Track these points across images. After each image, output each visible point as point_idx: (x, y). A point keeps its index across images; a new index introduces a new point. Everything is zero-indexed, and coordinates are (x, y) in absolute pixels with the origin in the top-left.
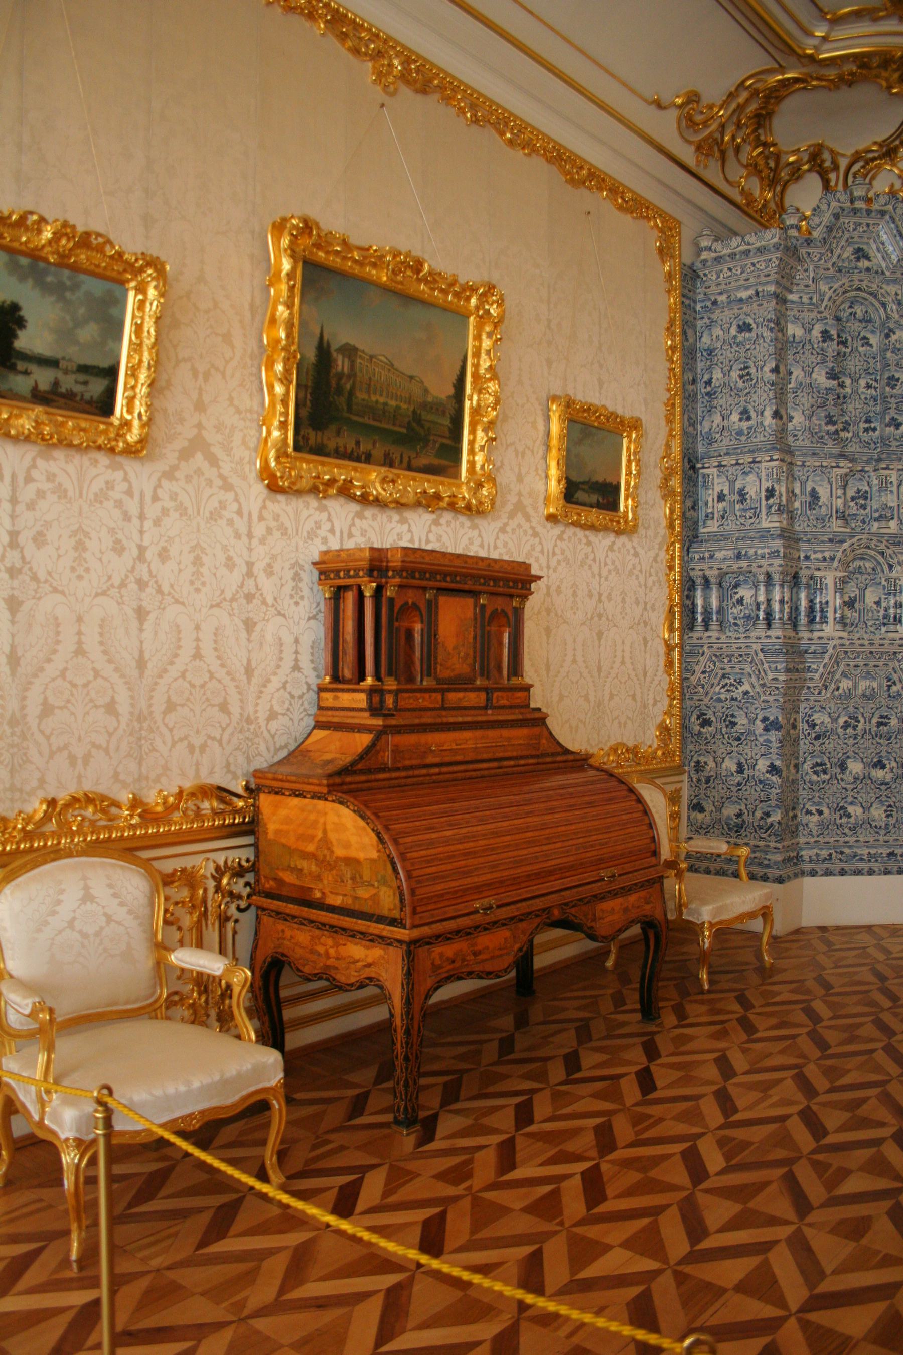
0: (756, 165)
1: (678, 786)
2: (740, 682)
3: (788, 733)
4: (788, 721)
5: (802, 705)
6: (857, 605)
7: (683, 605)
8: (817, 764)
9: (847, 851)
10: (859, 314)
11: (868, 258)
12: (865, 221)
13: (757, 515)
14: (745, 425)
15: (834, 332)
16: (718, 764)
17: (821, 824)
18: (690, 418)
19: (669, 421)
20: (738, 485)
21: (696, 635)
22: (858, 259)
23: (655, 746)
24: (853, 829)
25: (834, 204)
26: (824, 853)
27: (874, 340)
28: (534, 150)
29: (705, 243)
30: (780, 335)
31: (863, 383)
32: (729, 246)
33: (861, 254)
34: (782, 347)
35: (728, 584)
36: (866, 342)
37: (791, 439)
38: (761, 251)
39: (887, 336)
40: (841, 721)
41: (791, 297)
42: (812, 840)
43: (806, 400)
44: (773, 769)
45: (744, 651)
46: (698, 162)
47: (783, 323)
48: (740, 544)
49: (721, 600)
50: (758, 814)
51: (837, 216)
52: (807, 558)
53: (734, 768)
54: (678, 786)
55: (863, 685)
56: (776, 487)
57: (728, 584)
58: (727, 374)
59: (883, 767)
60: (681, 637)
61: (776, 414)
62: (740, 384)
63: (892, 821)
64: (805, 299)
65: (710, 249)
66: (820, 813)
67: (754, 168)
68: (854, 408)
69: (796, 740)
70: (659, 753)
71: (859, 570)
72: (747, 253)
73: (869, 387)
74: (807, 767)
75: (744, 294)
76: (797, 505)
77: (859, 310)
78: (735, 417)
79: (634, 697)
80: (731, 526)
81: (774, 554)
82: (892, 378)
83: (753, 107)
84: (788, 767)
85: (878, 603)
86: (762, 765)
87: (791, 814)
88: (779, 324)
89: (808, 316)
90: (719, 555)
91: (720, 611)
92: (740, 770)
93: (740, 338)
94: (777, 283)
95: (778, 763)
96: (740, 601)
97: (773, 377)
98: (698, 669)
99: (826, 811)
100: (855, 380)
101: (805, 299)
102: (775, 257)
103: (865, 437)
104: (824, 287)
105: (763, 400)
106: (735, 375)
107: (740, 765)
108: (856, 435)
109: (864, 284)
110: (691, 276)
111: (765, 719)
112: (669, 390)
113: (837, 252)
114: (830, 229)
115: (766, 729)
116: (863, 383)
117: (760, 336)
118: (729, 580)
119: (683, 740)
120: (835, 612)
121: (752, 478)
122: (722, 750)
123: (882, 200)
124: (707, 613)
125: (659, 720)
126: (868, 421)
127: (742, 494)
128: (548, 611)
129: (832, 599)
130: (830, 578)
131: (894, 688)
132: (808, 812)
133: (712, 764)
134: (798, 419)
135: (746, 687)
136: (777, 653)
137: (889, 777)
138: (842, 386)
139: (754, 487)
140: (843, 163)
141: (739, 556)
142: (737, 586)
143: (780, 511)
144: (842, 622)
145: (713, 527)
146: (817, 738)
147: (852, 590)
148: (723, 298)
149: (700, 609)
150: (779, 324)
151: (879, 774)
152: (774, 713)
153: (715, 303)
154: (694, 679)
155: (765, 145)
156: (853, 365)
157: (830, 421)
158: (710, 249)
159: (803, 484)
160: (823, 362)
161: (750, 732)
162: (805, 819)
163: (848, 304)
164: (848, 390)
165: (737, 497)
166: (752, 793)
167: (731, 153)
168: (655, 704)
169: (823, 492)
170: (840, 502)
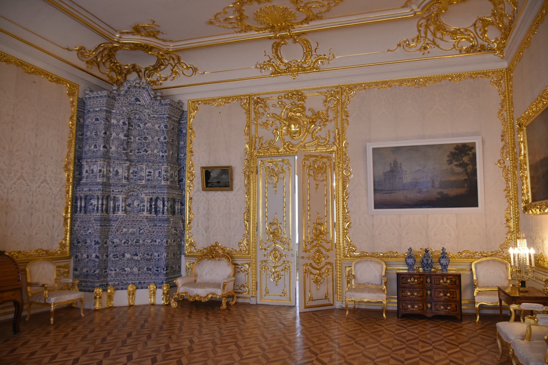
0: (112, 68)
1: (68, 263)
2: (88, 230)
3: (103, 245)
4: (103, 241)
5: (110, 237)
6: (131, 206)
7: (72, 205)
8: (114, 255)
9: (124, 282)
10: (137, 117)
11: (140, 101)
12: (138, 90)
13: (96, 178)
14: (95, 149)
15: (127, 123)
16: (82, 256)
17: (116, 274)
18: (79, 147)
19: (69, 147)
20: (92, 168)
21: (76, 214)
22: (136, 101)
23: (58, 249)
24: (127, 275)
25: (129, 84)
26: (117, 283)
27: (142, 125)
28: (10, 62)
29: (87, 92)
30: (108, 123)
31: (137, 138)
32: (102, 93)
33: (137, 100)
34: (108, 127)
35: (87, 198)
36: (139, 126)
37: (111, 154)
38: (101, 97)
39: (145, 125)
40: (123, 241)
41: (113, 111)
42: (112, 279)
43: (116, 143)
44: (97, 257)
45: (89, 220)
46: (88, 67)
47: (109, 119)
48: (91, 186)
49: (85, 204)
50: (92, 271)
51: (129, 88)
52: (113, 191)
53: (86, 257)
54: (68, 263)
55: (131, 230)
56: (102, 169)
57: (87, 198)
58: (91, 133)
59: (137, 255)
60: (71, 215)
61: (104, 147)
62: (95, 137)
63: (140, 272)
64: (118, 112)
65: (88, 94)
66: (116, 270)
67: (112, 69)
68: (134, 146)
69: (107, 247)
70: (59, 252)
71: (132, 195)
72: (97, 97)
73: (139, 139)
74: (111, 256)
75: (97, 109)
76: (111, 175)
77: (137, 116)
78: (93, 147)
79: (48, 234)
80: (89, 181)
81: (99, 190)
82: (146, 137)
83: (106, 52)
84: (102, 256)
85: (138, 205)
86: (94, 255)
87: (104, 271)
88: (107, 119)
89: (118, 117)
90: (85, 189)
91: (85, 207)
92: (88, 258)
93: (96, 123)
94: (106, 107)
95: (98, 255)
96: (91, 204)
97: (103, 135)
98: (76, 225)
99: (118, 270)
100: (135, 137)
101: (118, 112)
102: (105, 99)
103: (137, 155)
104: (124, 109)
105: (101, 142)
106: (93, 134)
107: (88, 255)
108: (134, 154)
109: (138, 109)
110: (82, 104)
111: (95, 241)
112: (70, 137)
113: (129, 99)
114: (126, 92)
115: (95, 244)
116: (137, 138)
117: (101, 123)
118: (88, 198)
119: (71, 248)
120: (122, 207)
121: (95, 166)
122: (83, 251)
123: (144, 84)
124: (81, 207)
125: (60, 242)
126: (139, 150)
127: (92, 171)
128: (7, 207)
129: (121, 204)
130: (121, 197)
131: (141, 231)
132: (112, 270)
133: (80, 256)
134: (113, 148)
135: (90, 231)
136: (98, 220)
137: (139, 258)
138: (130, 139)
139: (96, 169)
140: (143, 70)
141: (90, 190)
142: (91, 199)
143: (103, 176)
144: (125, 211)
145: (84, 181)
146: (115, 247)
147: (129, 201)
148: (91, 110)
149: (79, 206)
150: (107, 119)
151: (136, 258)
152: (97, 239)
153: (89, 111)
154: (75, 228)
155: (114, 63)
156: (134, 132)
157: (124, 149)
158: (88, 94)
159: (114, 168)
160: (123, 131)
161: (91, 245)
162: (110, 272)
163: (133, 114)
164: (132, 140)
165: (91, 172)
166: (91, 264)
167: (101, 64)
168: (58, 236)
169: (120, 171)
170: (126, 174)
